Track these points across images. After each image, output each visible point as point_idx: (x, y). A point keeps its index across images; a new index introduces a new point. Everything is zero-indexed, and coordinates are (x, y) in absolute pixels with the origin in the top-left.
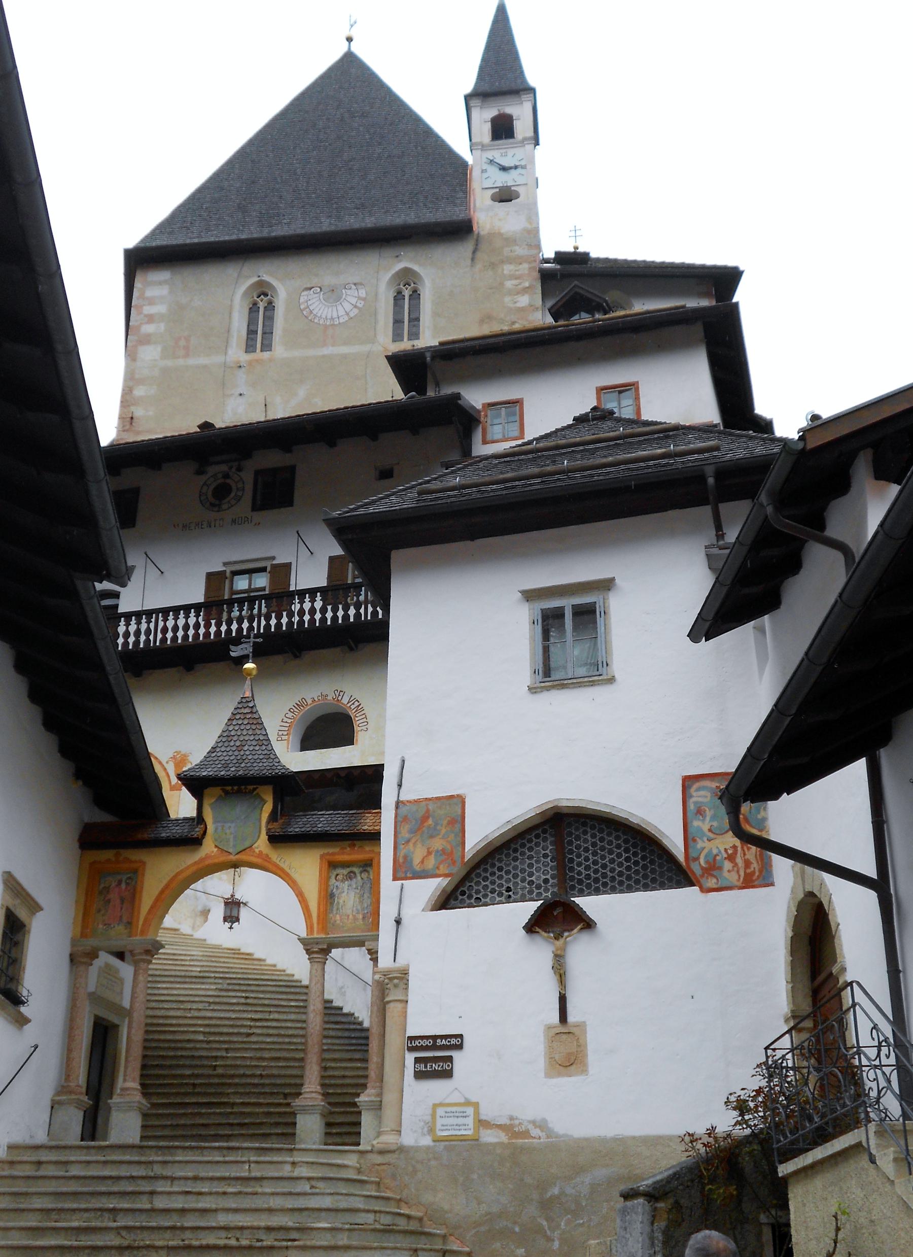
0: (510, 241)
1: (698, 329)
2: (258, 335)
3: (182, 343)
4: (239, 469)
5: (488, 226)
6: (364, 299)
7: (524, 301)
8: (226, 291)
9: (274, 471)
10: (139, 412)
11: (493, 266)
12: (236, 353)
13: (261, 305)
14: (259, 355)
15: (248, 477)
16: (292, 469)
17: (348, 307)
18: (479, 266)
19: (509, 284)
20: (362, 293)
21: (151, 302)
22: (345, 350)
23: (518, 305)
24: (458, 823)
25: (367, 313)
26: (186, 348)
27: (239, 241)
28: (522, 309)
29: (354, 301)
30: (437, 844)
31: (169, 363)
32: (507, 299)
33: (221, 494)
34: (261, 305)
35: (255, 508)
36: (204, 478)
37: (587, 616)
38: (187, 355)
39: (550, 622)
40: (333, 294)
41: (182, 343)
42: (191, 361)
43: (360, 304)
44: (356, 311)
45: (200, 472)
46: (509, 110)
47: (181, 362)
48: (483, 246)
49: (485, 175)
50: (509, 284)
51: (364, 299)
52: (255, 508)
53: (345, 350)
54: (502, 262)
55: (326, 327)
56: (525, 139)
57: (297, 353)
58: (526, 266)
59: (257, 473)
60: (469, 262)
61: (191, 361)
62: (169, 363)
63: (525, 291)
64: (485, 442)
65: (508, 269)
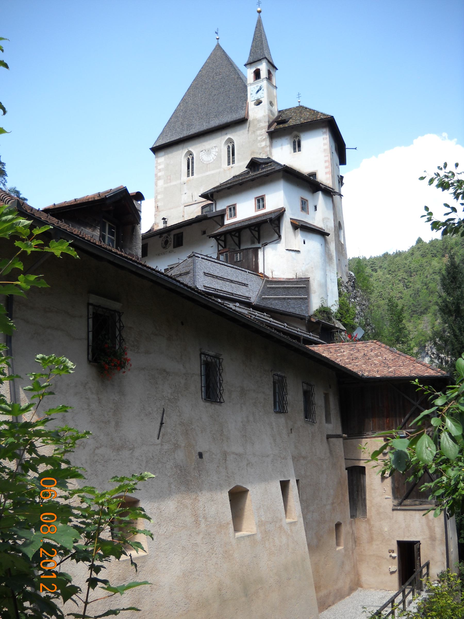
0: (259, 121)
1: (281, 174)
4: (169, 235)
5: (252, 117)
6: (217, 152)
7: (263, 144)
8: (178, 156)
9: (178, 234)
10: (159, 204)
12: (184, 178)
14: (191, 177)
15: (172, 237)
16: (182, 233)
18: (250, 133)
20: (217, 150)
22: (213, 172)
23: (262, 146)
25: (219, 157)
26: (170, 179)
27: (180, 138)
28: (263, 148)
29: (214, 153)
31: (166, 185)
32: (259, 144)
33: (166, 242)
36: (162, 238)
38: (170, 182)
40: (208, 152)
41: (169, 178)
42: (172, 184)
44: (215, 157)
45: (160, 237)
46: (259, 67)
47: (169, 184)
48: (251, 125)
49: (252, 96)
50: (259, 138)
51: (217, 152)
52: (174, 247)
53: (213, 172)
54: (257, 130)
55: (207, 164)
56: (263, 79)
58: (264, 130)
59: (174, 235)
60: (247, 132)
61: (172, 184)
62: (166, 185)
64: (227, 220)
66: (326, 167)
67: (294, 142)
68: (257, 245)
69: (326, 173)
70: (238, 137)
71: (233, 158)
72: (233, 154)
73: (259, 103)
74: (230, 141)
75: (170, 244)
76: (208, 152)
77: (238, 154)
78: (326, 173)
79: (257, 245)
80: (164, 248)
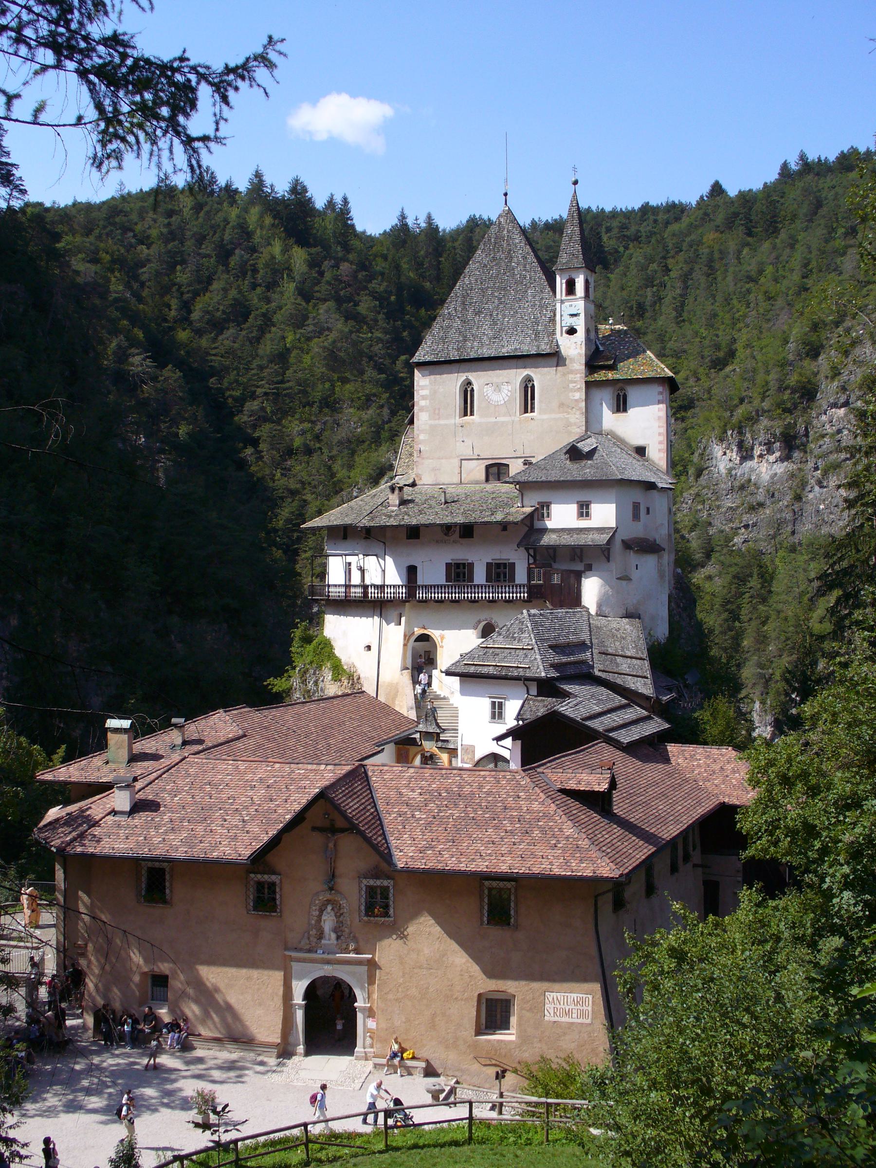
2: (467, 406)
3: (437, 412)
11: (564, 375)
13: (467, 393)
17: (504, 396)
18: (559, 375)
19: (571, 385)
21: (423, 388)
24: (474, 752)
26: (438, 414)
28: (576, 400)
30: (470, 756)
31: (432, 422)
32: (570, 394)
34: (467, 393)
35: (460, 537)
37: (500, 704)
38: (439, 419)
39: (493, 703)
40: (498, 388)
42: (442, 422)
43: (509, 394)
47: (437, 422)
52: (460, 537)
57: (484, 420)
58: (579, 375)
61: (442, 422)
62: (432, 422)
63: (579, 389)
65: (571, 377)
66: (660, 443)
67: (618, 396)
68: (579, 567)
69: (660, 450)
70: (542, 377)
71: (533, 404)
72: (533, 398)
73: (572, 331)
74: (528, 380)
75: (455, 531)
76: (498, 388)
77: (540, 402)
78: (660, 450)
79: (579, 567)
80: (446, 534)
